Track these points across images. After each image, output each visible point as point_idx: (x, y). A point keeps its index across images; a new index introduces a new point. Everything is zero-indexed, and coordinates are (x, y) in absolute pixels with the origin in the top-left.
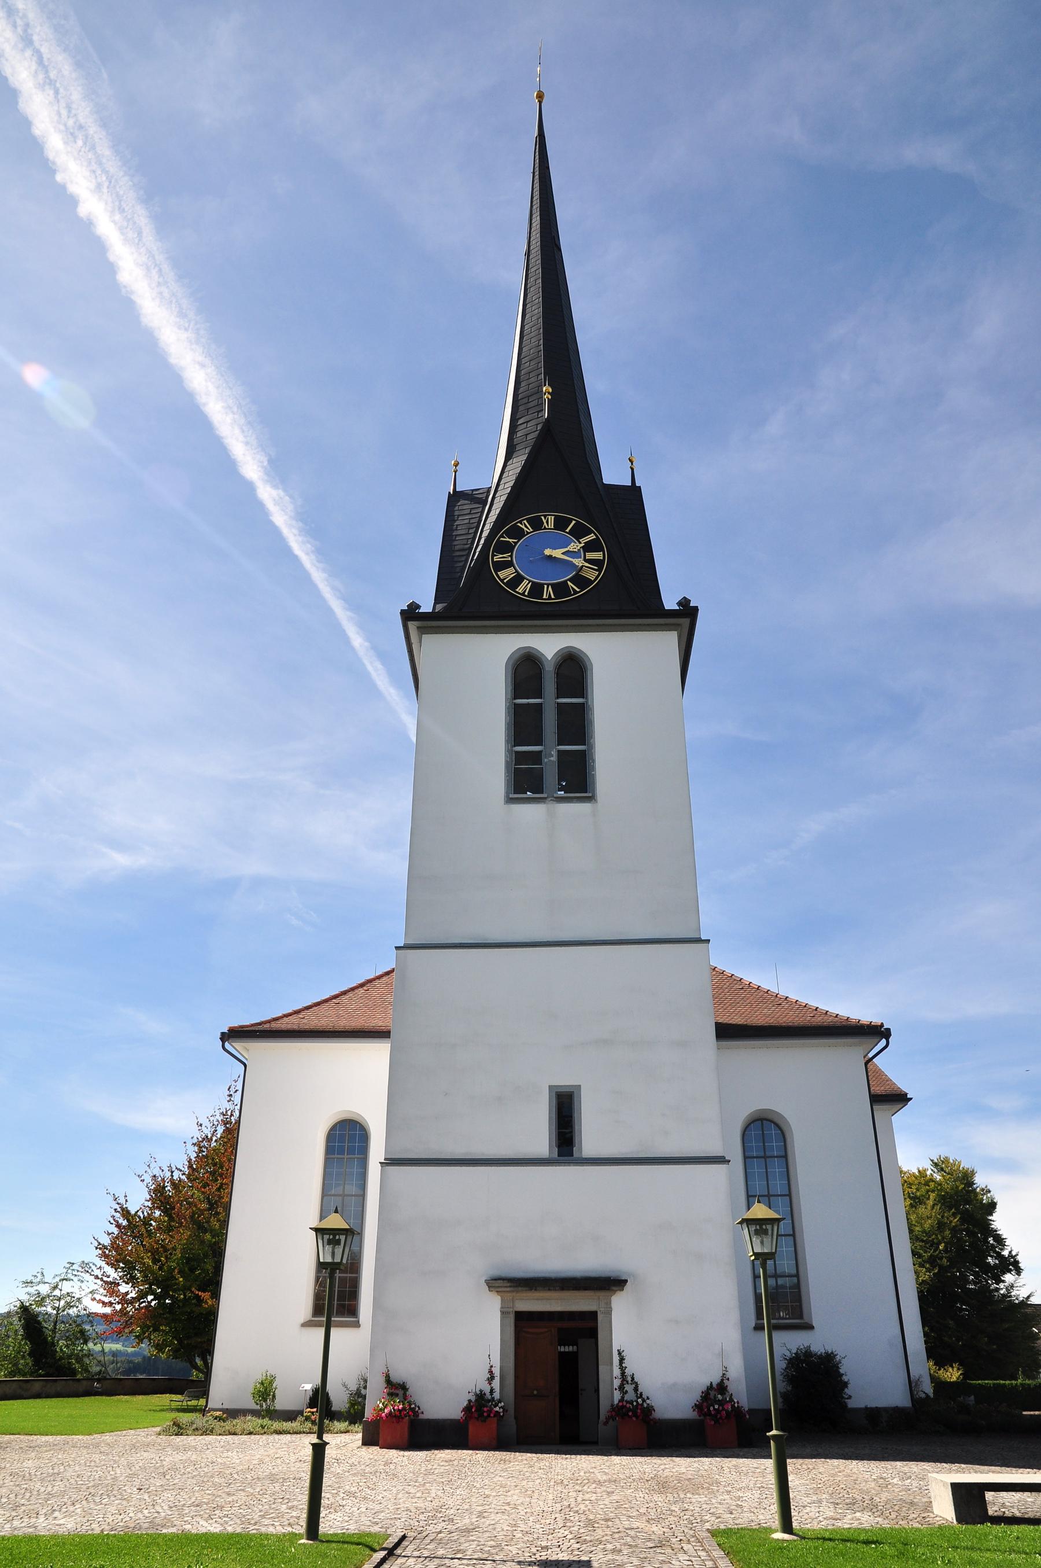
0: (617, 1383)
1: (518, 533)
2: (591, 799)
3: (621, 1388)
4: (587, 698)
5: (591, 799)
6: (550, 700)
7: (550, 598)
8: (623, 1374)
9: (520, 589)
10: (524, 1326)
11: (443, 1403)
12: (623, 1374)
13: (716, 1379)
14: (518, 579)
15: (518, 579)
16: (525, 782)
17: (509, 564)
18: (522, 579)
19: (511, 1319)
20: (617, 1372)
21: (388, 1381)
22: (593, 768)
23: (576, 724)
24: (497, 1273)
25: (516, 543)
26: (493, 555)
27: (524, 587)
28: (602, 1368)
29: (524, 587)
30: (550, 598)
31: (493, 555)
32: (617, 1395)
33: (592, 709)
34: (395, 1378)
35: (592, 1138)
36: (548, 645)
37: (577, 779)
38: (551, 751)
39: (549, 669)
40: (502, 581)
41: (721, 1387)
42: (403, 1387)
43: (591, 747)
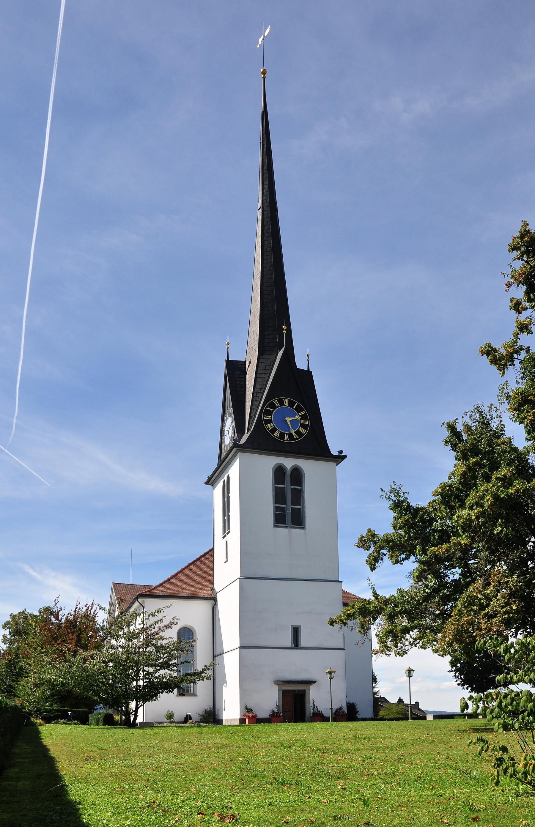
0: (312, 708)
1: (273, 406)
2: (304, 528)
3: (313, 709)
4: (302, 487)
5: (304, 528)
6: (288, 487)
7: (287, 440)
8: (314, 706)
9: (275, 434)
10: (285, 694)
11: (264, 713)
12: (314, 706)
13: (339, 707)
14: (274, 430)
15: (274, 430)
16: (280, 520)
17: (270, 422)
18: (276, 429)
19: (281, 692)
20: (312, 705)
21: (246, 708)
22: (305, 516)
23: (298, 497)
24: (276, 679)
25: (273, 411)
26: (264, 416)
27: (277, 434)
28: (307, 705)
29: (277, 434)
30: (287, 440)
31: (264, 416)
32: (312, 711)
33: (304, 492)
34: (248, 708)
35: (304, 641)
36: (289, 463)
37: (298, 520)
38: (289, 507)
39: (289, 473)
40: (268, 429)
41: (341, 709)
42: (251, 710)
43: (304, 508)
